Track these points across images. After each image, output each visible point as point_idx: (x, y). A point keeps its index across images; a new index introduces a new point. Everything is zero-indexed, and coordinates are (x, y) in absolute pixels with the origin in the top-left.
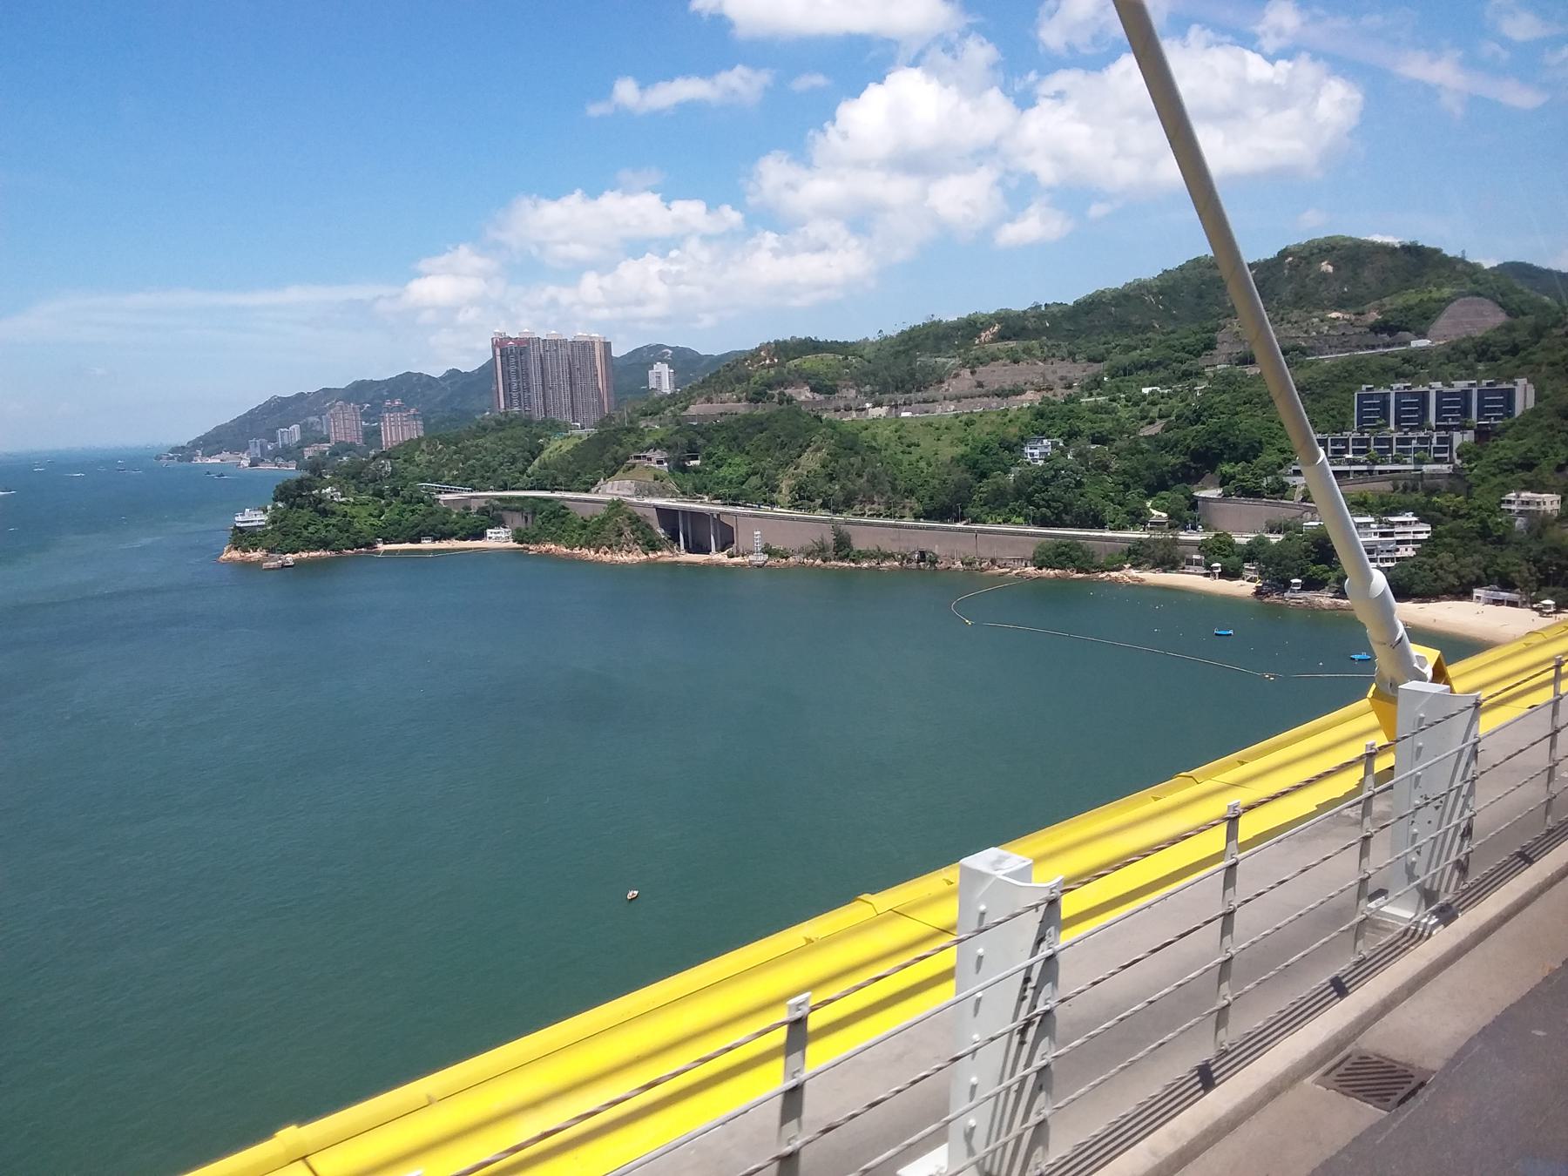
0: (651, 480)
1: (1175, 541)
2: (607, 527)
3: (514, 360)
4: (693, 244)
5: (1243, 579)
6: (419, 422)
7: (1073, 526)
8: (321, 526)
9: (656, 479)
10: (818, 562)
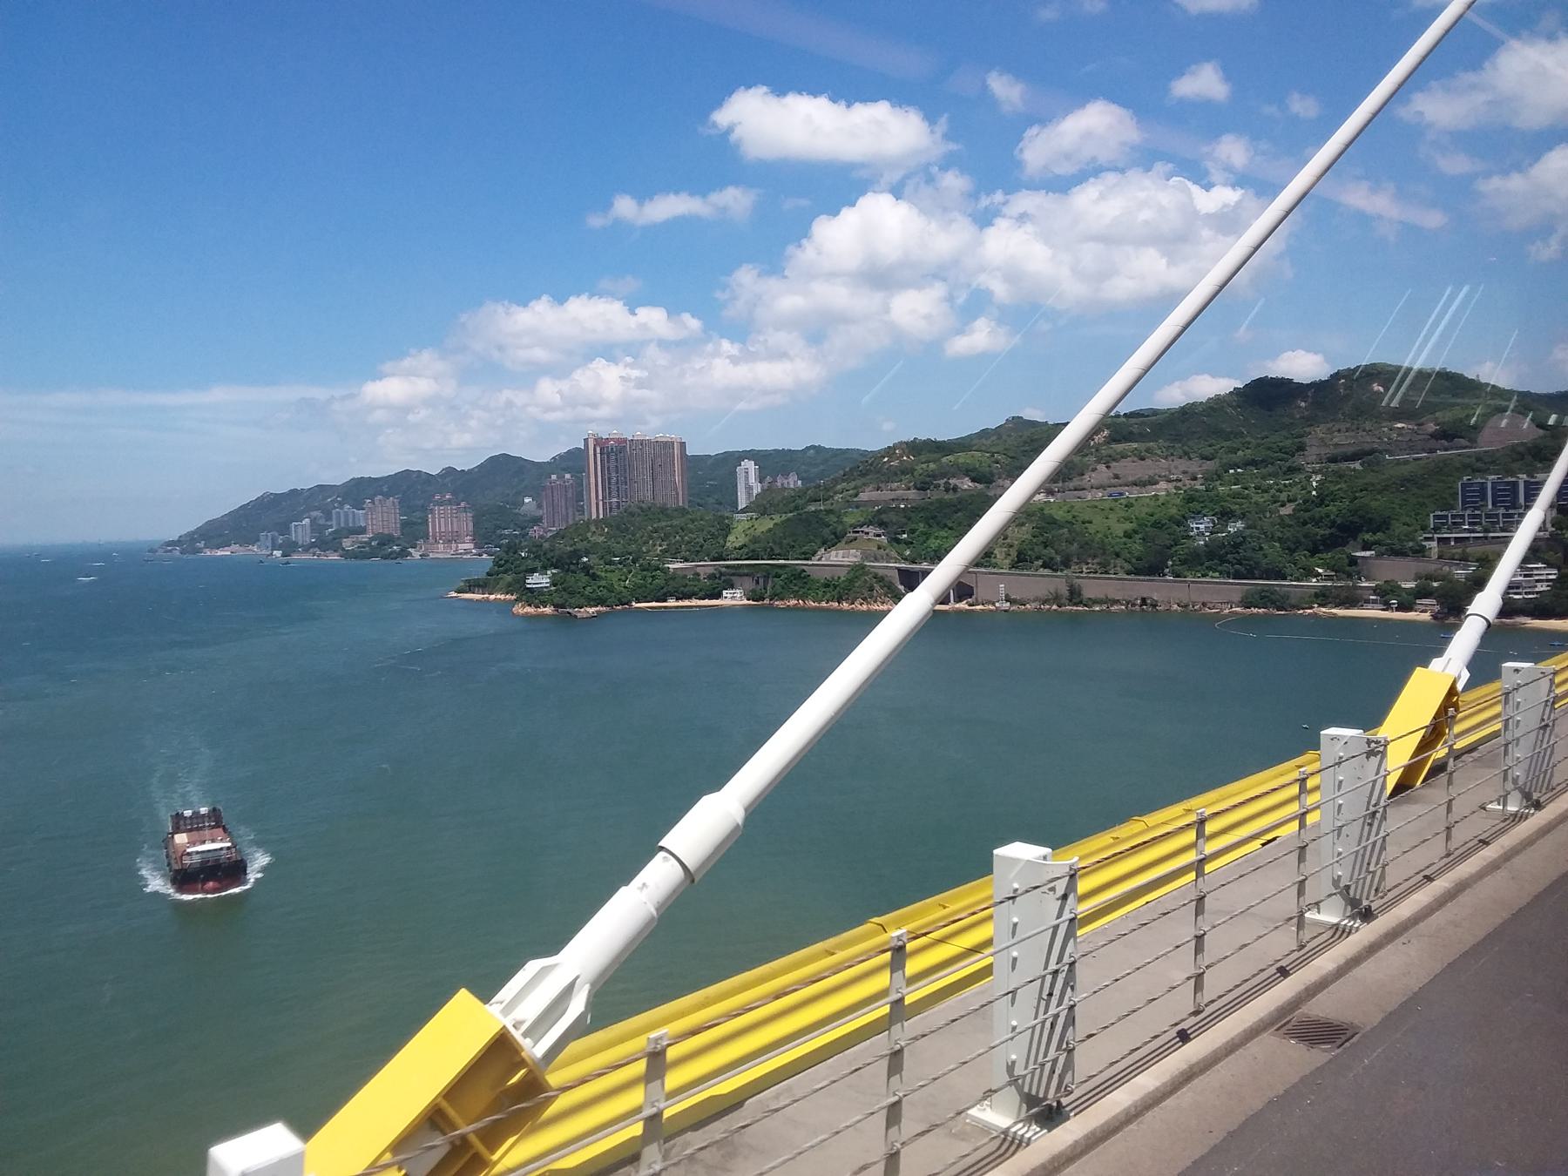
0: (875, 549)
1: (1356, 588)
2: (857, 585)
3: (614, 457)
4: (652, 351)
5: (1416, 611)
6: (469, 514)
7: (1261, 578)
8: (595, 587)
9: (879, 548)
10: (1055, 607)
